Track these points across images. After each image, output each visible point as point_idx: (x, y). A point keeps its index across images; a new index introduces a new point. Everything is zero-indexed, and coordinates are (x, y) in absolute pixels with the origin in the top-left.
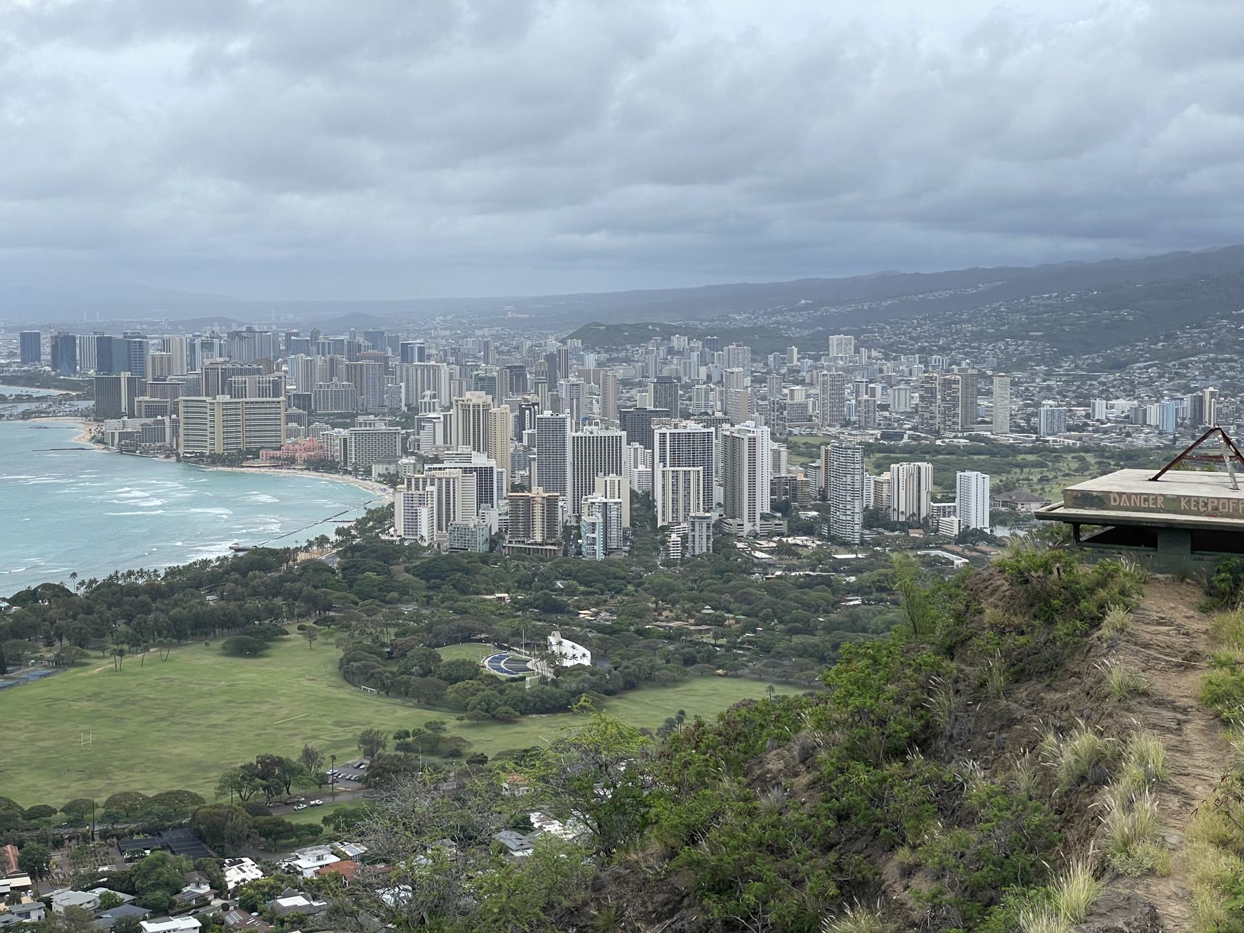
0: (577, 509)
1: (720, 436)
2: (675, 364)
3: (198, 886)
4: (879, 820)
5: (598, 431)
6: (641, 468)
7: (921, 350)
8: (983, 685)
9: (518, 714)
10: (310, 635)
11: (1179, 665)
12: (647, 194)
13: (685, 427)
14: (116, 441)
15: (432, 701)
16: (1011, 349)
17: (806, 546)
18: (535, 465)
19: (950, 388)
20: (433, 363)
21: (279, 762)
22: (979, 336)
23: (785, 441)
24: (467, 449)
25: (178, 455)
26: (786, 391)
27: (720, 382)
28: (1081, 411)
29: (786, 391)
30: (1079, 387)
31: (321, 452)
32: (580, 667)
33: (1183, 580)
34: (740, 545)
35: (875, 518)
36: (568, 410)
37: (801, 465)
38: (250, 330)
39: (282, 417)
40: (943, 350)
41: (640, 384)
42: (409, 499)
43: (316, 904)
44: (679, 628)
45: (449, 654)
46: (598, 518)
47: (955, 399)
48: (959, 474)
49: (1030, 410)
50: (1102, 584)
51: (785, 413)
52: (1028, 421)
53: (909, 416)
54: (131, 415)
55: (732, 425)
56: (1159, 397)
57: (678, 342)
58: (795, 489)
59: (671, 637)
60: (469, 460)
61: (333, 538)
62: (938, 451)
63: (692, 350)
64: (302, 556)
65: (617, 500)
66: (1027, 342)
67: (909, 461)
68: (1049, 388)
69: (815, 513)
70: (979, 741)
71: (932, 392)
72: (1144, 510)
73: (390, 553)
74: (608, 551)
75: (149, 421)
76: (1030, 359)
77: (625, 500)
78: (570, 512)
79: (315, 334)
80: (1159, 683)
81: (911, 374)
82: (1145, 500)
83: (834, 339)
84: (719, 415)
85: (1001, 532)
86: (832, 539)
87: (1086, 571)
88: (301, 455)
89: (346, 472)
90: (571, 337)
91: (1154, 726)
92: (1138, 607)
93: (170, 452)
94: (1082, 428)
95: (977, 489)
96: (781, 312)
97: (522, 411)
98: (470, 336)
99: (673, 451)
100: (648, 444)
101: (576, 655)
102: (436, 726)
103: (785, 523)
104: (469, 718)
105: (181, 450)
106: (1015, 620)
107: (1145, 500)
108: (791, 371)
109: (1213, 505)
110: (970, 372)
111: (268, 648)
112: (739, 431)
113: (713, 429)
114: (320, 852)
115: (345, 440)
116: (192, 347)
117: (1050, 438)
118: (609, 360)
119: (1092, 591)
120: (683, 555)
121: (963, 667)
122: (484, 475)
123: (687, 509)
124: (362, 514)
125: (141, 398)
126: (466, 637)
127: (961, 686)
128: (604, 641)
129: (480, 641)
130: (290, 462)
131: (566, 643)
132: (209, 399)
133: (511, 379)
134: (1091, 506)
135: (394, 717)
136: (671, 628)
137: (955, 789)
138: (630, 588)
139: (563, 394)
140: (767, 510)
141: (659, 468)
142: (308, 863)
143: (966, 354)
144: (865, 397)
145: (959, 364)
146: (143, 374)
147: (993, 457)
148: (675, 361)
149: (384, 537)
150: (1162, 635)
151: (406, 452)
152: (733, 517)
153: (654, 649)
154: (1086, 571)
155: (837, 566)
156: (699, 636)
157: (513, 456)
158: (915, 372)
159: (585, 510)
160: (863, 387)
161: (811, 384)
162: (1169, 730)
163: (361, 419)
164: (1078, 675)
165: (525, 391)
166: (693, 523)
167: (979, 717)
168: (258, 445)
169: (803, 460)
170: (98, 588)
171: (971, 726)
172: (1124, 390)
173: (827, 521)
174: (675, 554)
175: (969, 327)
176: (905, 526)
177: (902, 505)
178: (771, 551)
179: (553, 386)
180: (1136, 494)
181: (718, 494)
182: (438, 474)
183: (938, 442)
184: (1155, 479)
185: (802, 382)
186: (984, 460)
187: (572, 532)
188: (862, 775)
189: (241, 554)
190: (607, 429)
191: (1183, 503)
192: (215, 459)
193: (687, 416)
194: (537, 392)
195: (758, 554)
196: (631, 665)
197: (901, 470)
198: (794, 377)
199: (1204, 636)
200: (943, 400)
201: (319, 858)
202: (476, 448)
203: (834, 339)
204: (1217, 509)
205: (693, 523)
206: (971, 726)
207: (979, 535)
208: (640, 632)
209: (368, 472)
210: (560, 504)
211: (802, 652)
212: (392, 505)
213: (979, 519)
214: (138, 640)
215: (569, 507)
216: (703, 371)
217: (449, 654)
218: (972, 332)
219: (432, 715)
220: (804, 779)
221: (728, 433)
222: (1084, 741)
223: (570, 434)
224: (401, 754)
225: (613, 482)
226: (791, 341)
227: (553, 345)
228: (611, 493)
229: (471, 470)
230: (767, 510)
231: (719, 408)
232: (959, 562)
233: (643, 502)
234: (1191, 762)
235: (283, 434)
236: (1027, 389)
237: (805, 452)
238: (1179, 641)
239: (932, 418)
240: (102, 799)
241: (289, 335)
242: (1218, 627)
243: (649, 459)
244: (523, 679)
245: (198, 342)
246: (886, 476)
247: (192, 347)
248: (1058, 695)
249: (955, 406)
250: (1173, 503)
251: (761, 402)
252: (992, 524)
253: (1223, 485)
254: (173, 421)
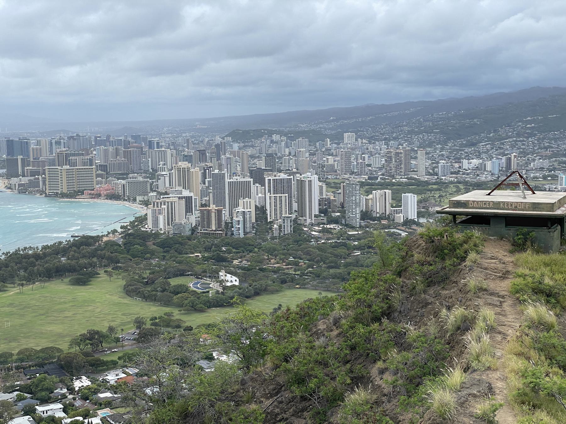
0: (231, 214)
1: (295, 180)
2: (274, 147)
3: (61, 390)
4: (368, 350)
5: (240, 179)
6: (260, 195)
7: (385, 139)
8: (414, 288)
9: (206, 308)
10: (110, 275)
11: (500, 277)
12: (231, 65)
13: (279, 176)
14: (17, 188)
15: (167, 303)
16: (425, 138)
17: (335, 229)
18: (211, 195)
19: (398, 156)
20: (163, 149)
21: (97, 333)
22: (411, 132)
23: (324, 182)
24: (180, 188)
25: (46, 194)
26: (325, 159)
27: (295, 155)
28: (457, 165)
29: (325, 159)
30: (456, 154)
31: (112, 191)
32: (234, 286)
33: (502, 239)
34: (305, 229)
35: (366, 215)
36: (226, 170)
37: (332, 192)
38: (78, 135)
39: (94, 175)
40: (395, 139)
41: (258, 157)
42: (154, 212)
43: (116, 396)
44: (278, 267)
45: (174, 282)
46: (241, 218)
47: (401, 161)
48: (403, 195)
49: (434, 165)
50: (465, 242)
51: (325, 169)
52: (433, 170)
53: (380, 169)
54: (24, 176)
55: (301, 175)
56: (491, 158)
57: (275, 137)
58: (329, 203)
59: (275, 271)
60: (181, 192)
61: (120, 230)
62: (393, 184)
63: (282, 141)
64: (105, 239)
65: (249, 210)
66: (432, 134)
67: (381, 189)
68: (443, 155)
69: (339, 214)
70: (413, 313)
71: (390, 158)
72: (485, 208)
73: (146, 237)
74: (245, 233)
75: (32, 178)
76: (434, 142)
77: (253, 210)
78: (228, 216)
79: (108, 137)
80: (492, 285)
81: (381, 150)
82: (485, 204)
83: (346, 135)
84: (294, 170)
85: (422, 220)
86: (346, 225)
87: (459, 236)
88: (103, 193)
89: (124, 200)
90: (226, 136)
91: (490, 304)
92: (482, 252)
93: (42, 192)
94: (457, 173)
95: (411, 201)
96: (322, 123)
97: (205, 170)
98: (181, 136)
99: (274, 187)
100: (263, 185)
101: (232, 280)
102: (169, 314)
103: (325, 218)
104: (184, 310)
105: (47, 192)
106: (428, 259)
107: (485, 204)
108: (327, 150)
109: (515, 206)
110: (407, 148)
111: (90, 281)
112: (304, 177)
113: (292, 177)
114: (117, 373)
115: (124, 185)
116: (51, 144)
117: (443, 178)
118: (244, 146)
119: (461, 245)
120: (280, 234)
121: (405, 280)
122: (188, 200)
123: (281, 214)
124: (132, 219)
125: (28, 168)
126: (182, 274)
127: (404, 289)
128: (244, 274)
129: (188, 275)
130: (98, 196)
131: (228, 275)
132: (60, 168)
133: (200, 156)
134: (461, 207)
135: (149, 311)
136: (275, 267)
137: (402, 335)
138: (256, 250)
139: (224, 162)
140: (317, 213)
141: (268, 195)
142: (112, 377)
143: (405, 140)
144: (361, 161)
145: (402, 145)
146: (28, 156)
147: (418, 187)
148: (274, 146)
149: (143, 229)
150: (493, 263)
151: (152, 190)
152: (302, 217)
153: (268, 277)
154: (459, 236)
155: (349, 238)
156: (287, 271)
157: (201, 191)
158: (382, 149)
159: (235, 215)
160: (359, 158)
161: (336, 155)
162: (496, 306)
163: (131, 175)
164: (456, 282)
165: (206, 161)
166: (284, 220)
167: (413, 302)
168: (83, 188)
169: (333, 190)
170: (10, 256)
171: (409, 307)
172: (476, 155)
173: (344, 217)
174: (276, 234)
175: (406, 128)
176: (380, 219)
177: (378, 209)
178: (319, 232)
179: (219, 159)
180: (481, 201)
181: (295, 206)
182: (167, 200)
183: (394, 181)
184: (489, 194)
185: (332, 155)
186: (414, 188)
187: (229, 225)
188: (361, 329)
189: (77, 239)
190: (244, 178)
191: (501, 205)
192: (63, 195)
193: (280, 171)
194: (211, 162)
195: (313, 233)
196: (256, 284)
197: (377, 193)
198: (328, 152)
199: (511, 264)
200: (396, 161)
201: (117, 375)
202: (184, 188)
203: (346, 135)
204: (516, 207)
205: (284, 220)
206: (409, 307)
207: (413, 222)
208: (261, 270)
209: (135, 200)
210: (223, 212)
211: (334, 277)
212: (146, 215)
213: (412, 215)
214: (30, 279)
215: (227, 213)
216: (287, 151)
217: (174, 282)
218: (408, 130)
219: (167, 310)
220: (335, 332)
221: (299, 179)
222: (458, 312)
223: (227, 180)
224: (153, 327)
225: (247, 202)
226: (326, 136)
227: (218, 140)
228: (246, 207)
229: (182, 198)
230: (317, 213)
231: (295, 167)
232: (404, 234)
233: (261, 211)
234: (506, 320)
235: (95, 183)
236: (433, 156)
237: (334, 186)
238: (500, 266)
239: (390, 170)
240: (15, 352)
241: (96, 137)
242: (517, 260)
243: (263, 191)
244: (208, 292)
245: (53, 141)
246: (370, 196)
247: (51, 144)
248: (447, 292)
249: (401, 164)
250: (497, 205)
251: (314, 164)
252: (418, 217)
253: (519, 196)
254: (43, 178)
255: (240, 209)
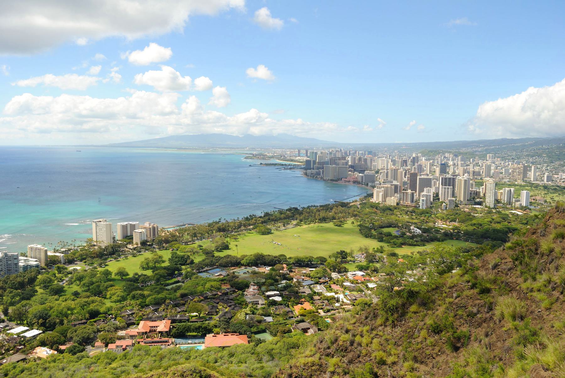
0: (419, 196)
21: (344, 252)
42: (377, 192)
46: (424, 198)
62: (515, 185)
64: (351, 204)
77: (432, 194)
122: (396, 187)
123: (448, 197)
187: (417, 202)
198: (477, 164)
209: (367, 185)
217: (386, 230)
223: (418, 177)
227: (414, 155)
255: (424, 193)
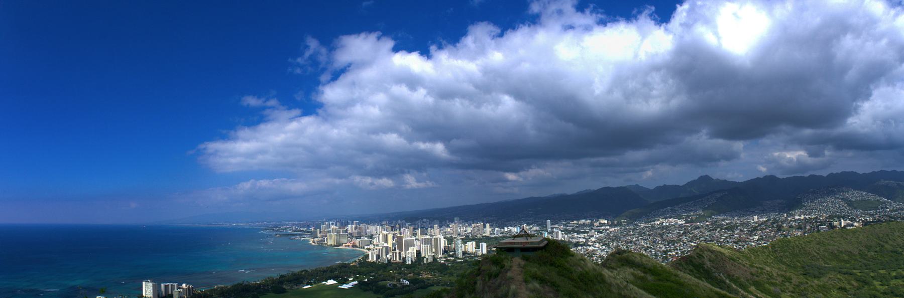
45: (381, 283)
122: (387, 248)
213: (485, 252)
233: (419, 253)
